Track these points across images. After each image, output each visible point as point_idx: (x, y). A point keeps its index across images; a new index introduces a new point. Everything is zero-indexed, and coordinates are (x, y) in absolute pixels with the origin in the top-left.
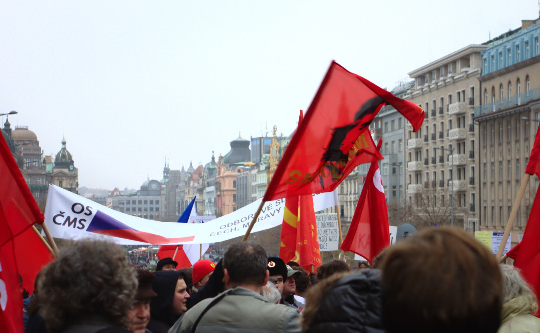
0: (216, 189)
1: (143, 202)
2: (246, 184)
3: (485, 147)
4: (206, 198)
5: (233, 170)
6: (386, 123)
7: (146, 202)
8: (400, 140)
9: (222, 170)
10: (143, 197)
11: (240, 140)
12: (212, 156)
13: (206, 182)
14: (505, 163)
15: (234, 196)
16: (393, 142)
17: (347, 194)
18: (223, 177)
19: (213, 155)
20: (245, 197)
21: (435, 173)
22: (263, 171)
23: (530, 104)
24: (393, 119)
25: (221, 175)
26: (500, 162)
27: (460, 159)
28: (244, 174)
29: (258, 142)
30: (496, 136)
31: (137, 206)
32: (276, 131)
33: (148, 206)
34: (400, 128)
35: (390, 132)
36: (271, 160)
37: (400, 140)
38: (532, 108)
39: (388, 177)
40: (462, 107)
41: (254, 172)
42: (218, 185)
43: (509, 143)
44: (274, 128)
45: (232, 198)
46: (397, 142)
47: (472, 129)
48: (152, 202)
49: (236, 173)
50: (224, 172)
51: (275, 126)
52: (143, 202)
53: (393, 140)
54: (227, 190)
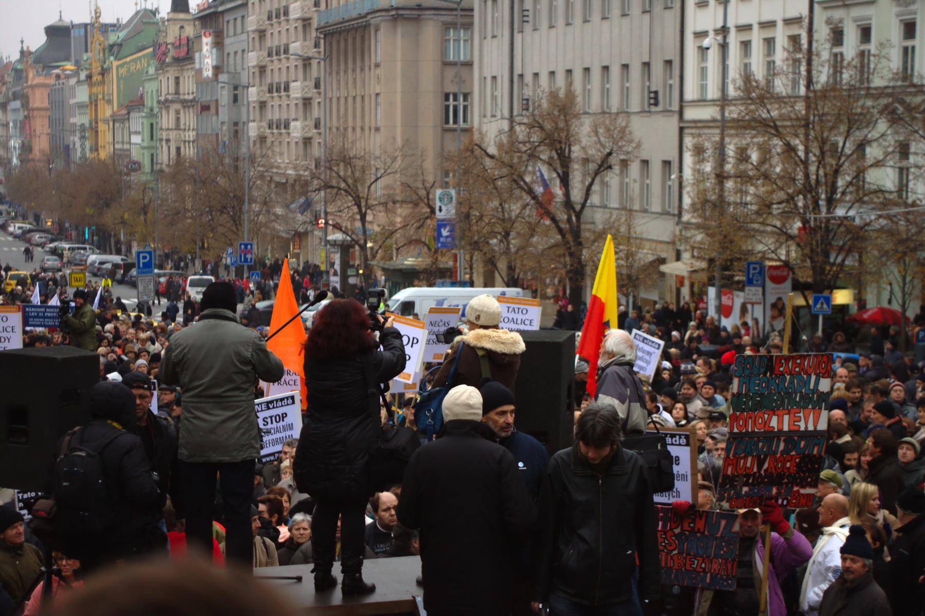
0: (23, 106)
2: (63, 101)
3: (330, 74)
4: (11, 117)
5: (48, 75)
6: (228, 22)
8: (243, 51)
9: (31, 75)
11: (60, 24)
12: (20, 49)
13: (10, 93)
14: (350, 100)
16: (236, 53)
17: (185, 130)
18: (32, 87)
19: (22, 47)
21: (280, 105)
22: (83, 81)
23: (369, 17)
24: (235, 17)
25: (29, 83)
26: (346, 98)
27: (303, 90)
29: (82, 31)
30: (342, 58)
32: (99, 17)
34: (242, 33)
35: (231, 37)
36: (94, 66)
37: (243, 51)
38: (372, 21)
39: (226, 107)
40: (306, 10)
41: (73, 81)
42: (25, 99)
43: (354, 70)
44: (96, 13)
46: (240, 53)
47: (317, 45)
49: (52, 81)
50: (33, 79)
51: (98, 8)
53: (235, 50)
54: (38, 109)
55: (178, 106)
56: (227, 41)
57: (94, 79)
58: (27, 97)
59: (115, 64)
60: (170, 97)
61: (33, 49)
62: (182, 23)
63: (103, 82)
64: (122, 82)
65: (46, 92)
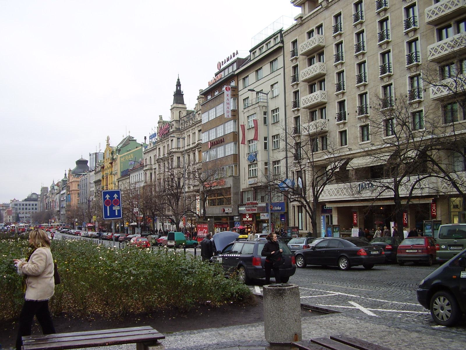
0: (67, 190)
1: (28, 205)
7: (29, 205)
9: (71, 178)
10: (28, 202)
12: (65, 173)
15: (79, 194)
18: (71, 182)
20: (85, 185)
25: (70, 181)
28: (85, 177)
31: (25, 207)
33: (31, 207)
45: (77, 195)
48: (33, 205)
52: (28, 205)
55: (179, 155)
56: (240, 93)
57: (105, 167)
58: (69, 187)
59: (119, 156)
60: (174, 150)
61: (72, 170)
62: (180, 109)
63: (112, 167)
64: (122, 164)
65: (77, 184)
